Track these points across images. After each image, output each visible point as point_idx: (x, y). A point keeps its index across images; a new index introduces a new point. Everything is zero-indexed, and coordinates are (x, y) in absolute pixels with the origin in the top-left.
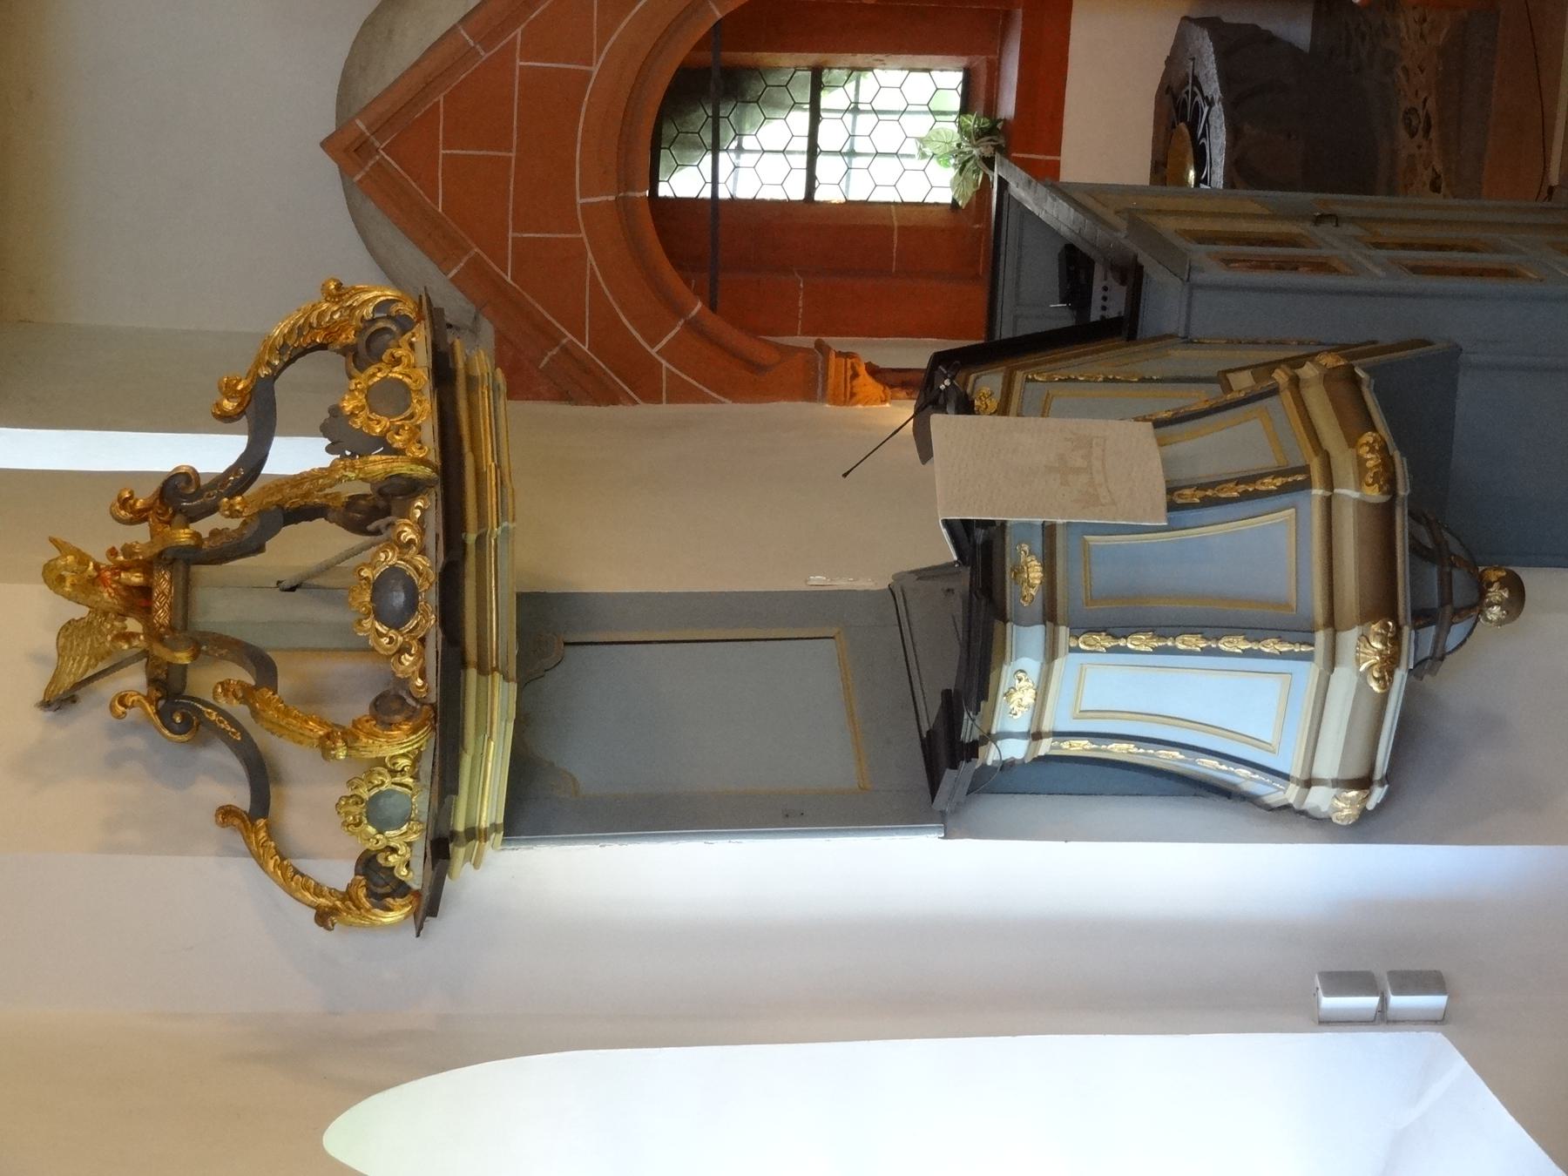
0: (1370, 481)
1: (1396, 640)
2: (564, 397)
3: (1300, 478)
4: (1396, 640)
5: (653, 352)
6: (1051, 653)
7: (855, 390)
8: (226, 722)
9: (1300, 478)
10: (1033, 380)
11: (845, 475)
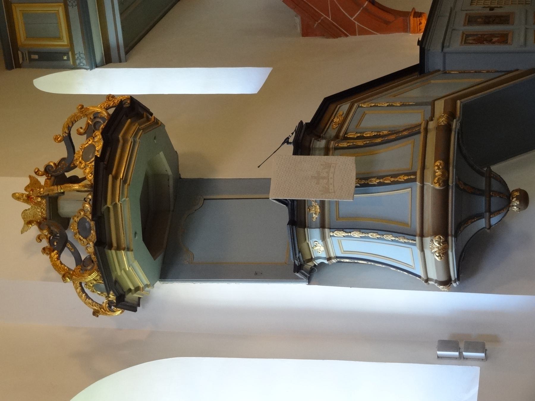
0: (436, 181)
1: (446, 242)
2: (323, 35)
3: (412, 177)
4: (446, 242)
5: (352, 19)
6: (323, 238)
7: (420, 28)
8: (70, 245)
9: (412, 177)
10: (362, 107)
11: (259, 167)
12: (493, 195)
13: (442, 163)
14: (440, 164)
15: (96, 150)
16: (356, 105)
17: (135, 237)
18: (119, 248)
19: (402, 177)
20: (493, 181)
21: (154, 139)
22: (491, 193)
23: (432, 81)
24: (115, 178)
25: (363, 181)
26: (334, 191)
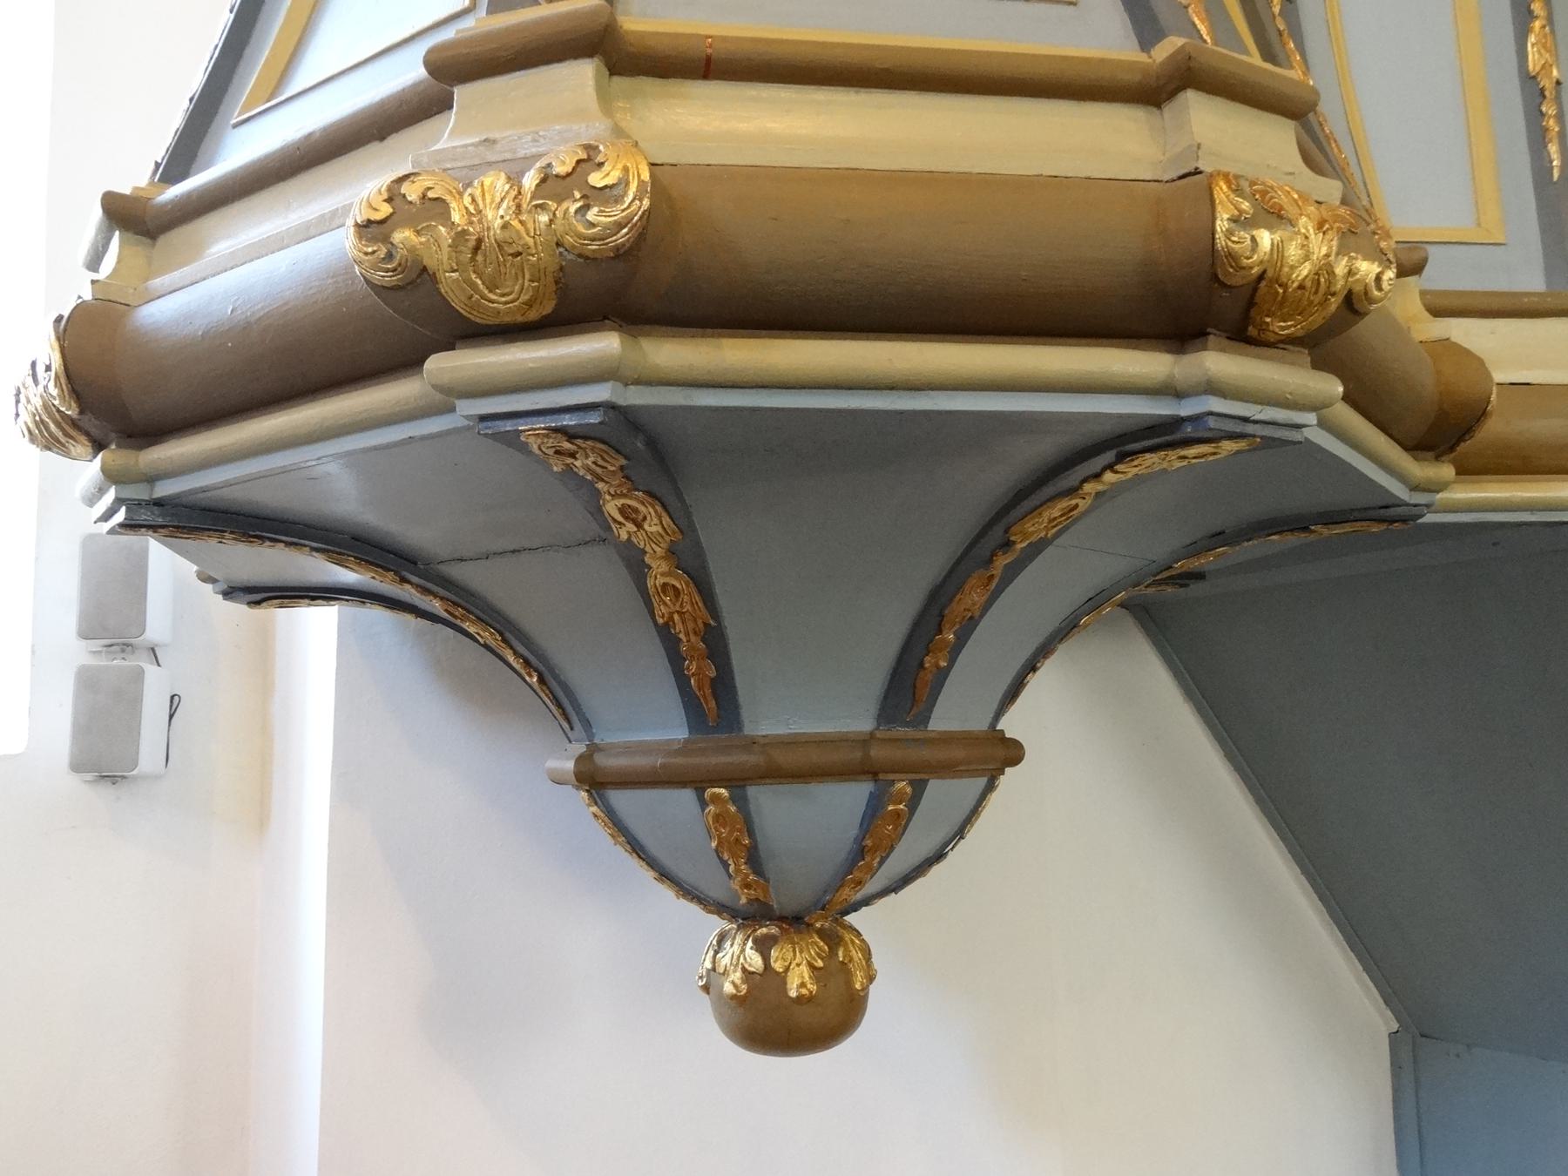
12: (711, 808)
13: (616, 213)
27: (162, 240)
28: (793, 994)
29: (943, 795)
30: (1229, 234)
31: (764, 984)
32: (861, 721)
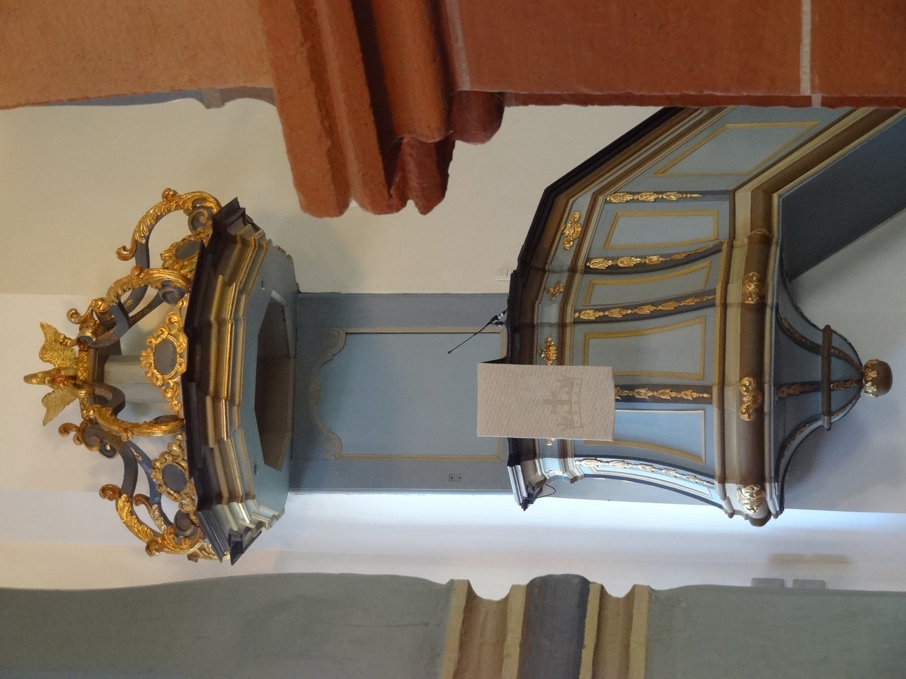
0: (744, 411)
10: (610, 202)
11: (449, 352)
12: (835, 388)
13: (753, 382)
14: (750, 385)
15: (177, 352)
16: (601, 199)
17: (256, 473)
18: (233, 497)
19: (689, 392)
20: (835, 362)
21: (262, 287)
22: (832, 385)
23: (729, 126)
24: (216, 398)
25: (626, 391)
26: (582, 424)
27: (727, 477)
28: (876, 376)
29: (836, 342)
30: (752, 300)
31: (875, 382)
32: (819, 359)
